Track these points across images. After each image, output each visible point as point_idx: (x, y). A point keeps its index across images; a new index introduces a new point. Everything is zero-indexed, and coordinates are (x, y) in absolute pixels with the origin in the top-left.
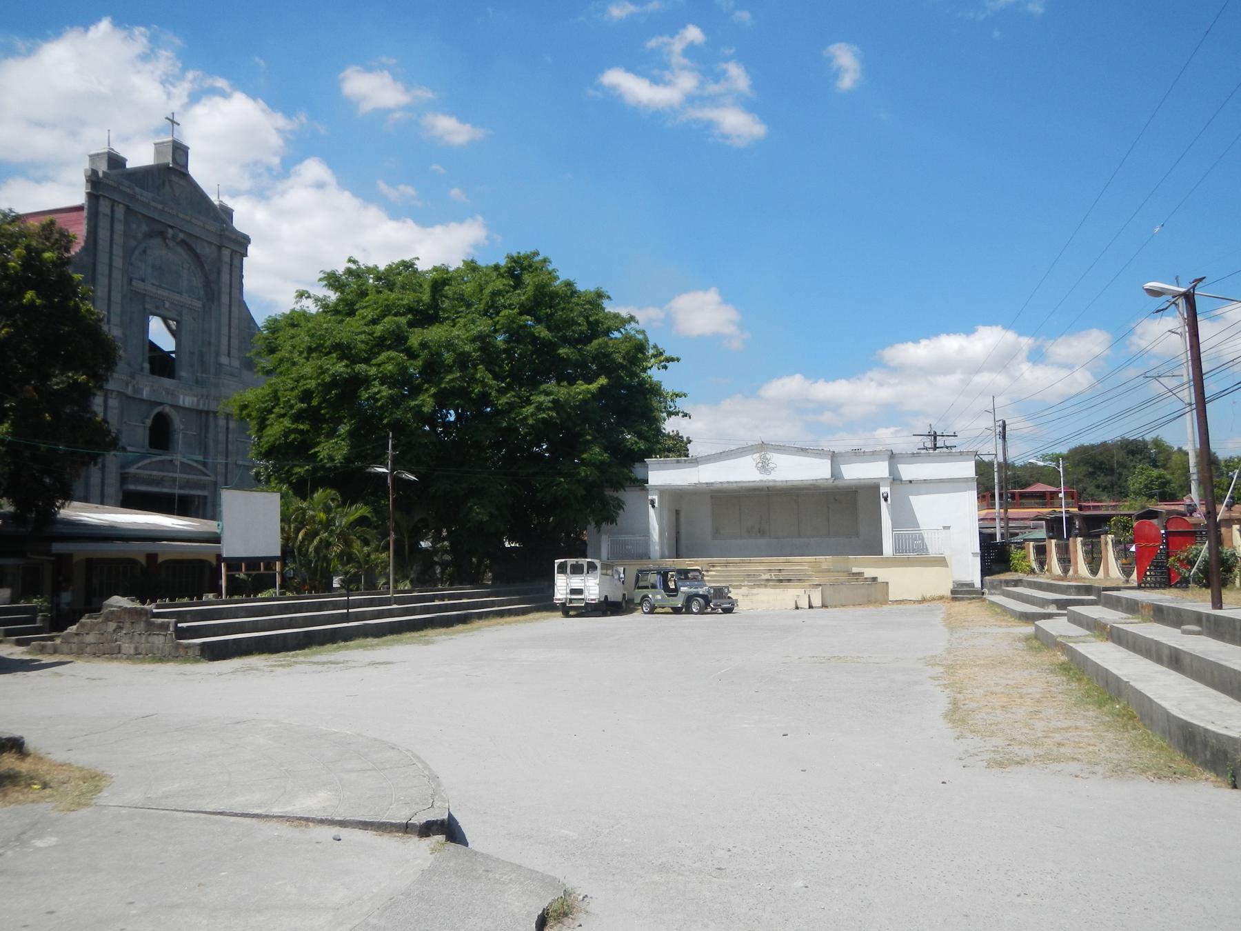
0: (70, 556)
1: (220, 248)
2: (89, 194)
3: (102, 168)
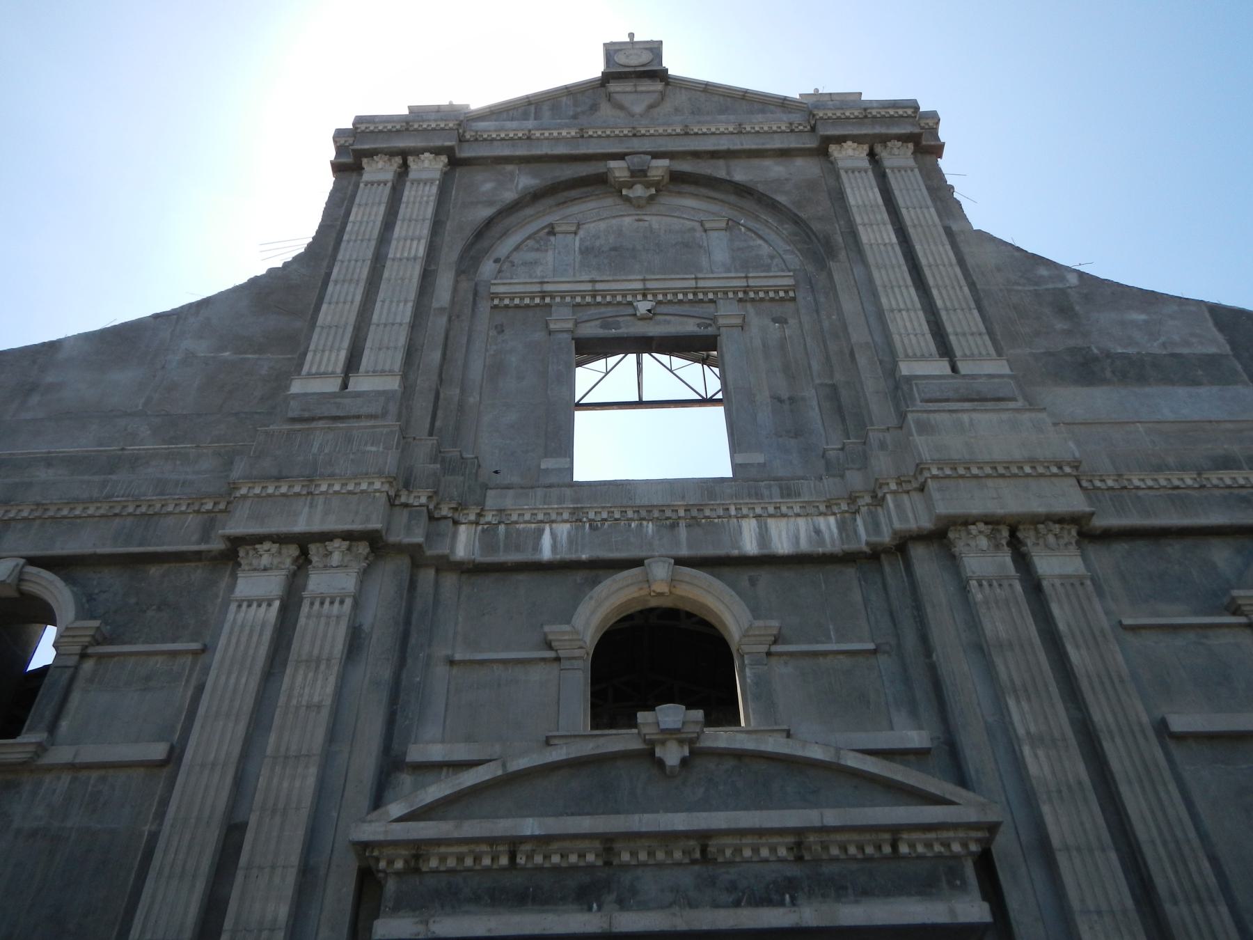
1: (822, 151)
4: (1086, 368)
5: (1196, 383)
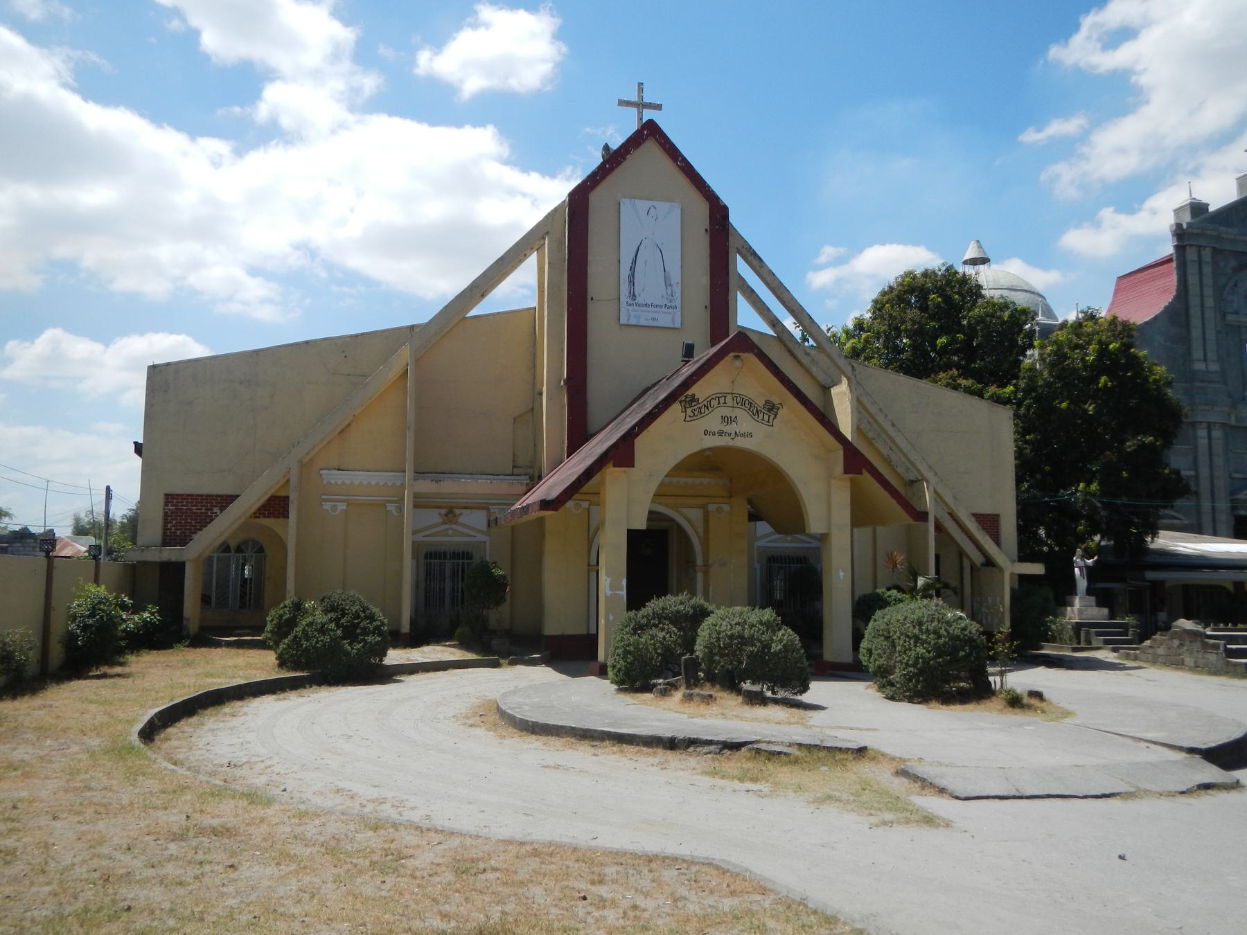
0: (1162, 582)
2: (1176, 247)
3: (1187, 218)
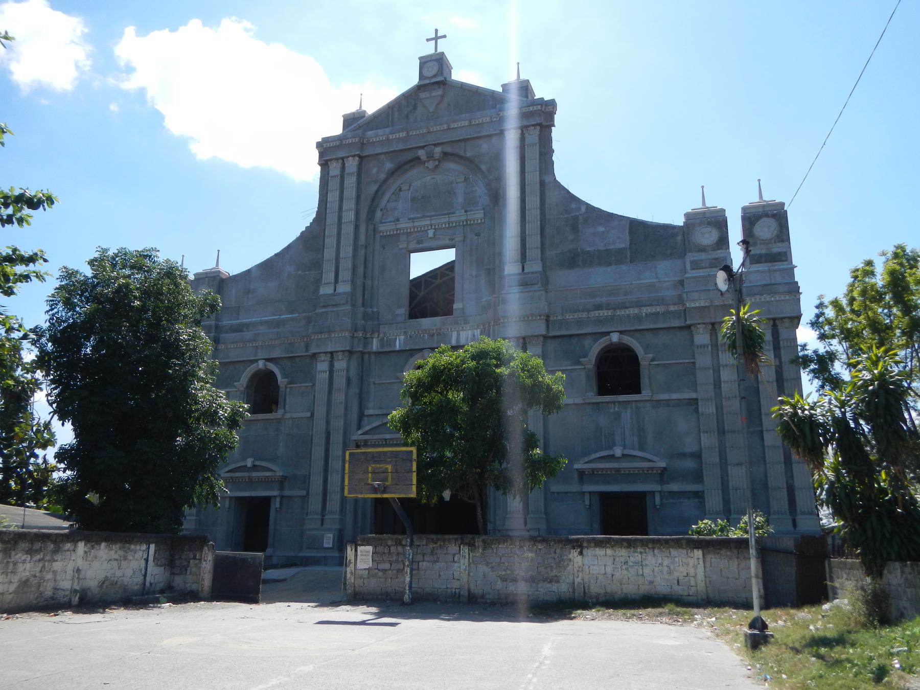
4: (573, 260)
5: (610, 264)
